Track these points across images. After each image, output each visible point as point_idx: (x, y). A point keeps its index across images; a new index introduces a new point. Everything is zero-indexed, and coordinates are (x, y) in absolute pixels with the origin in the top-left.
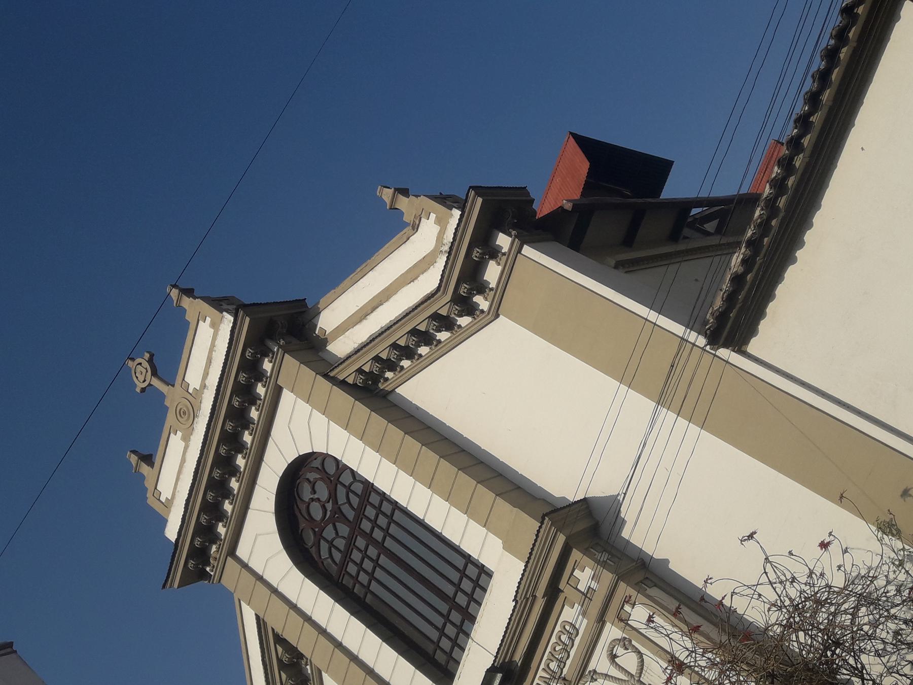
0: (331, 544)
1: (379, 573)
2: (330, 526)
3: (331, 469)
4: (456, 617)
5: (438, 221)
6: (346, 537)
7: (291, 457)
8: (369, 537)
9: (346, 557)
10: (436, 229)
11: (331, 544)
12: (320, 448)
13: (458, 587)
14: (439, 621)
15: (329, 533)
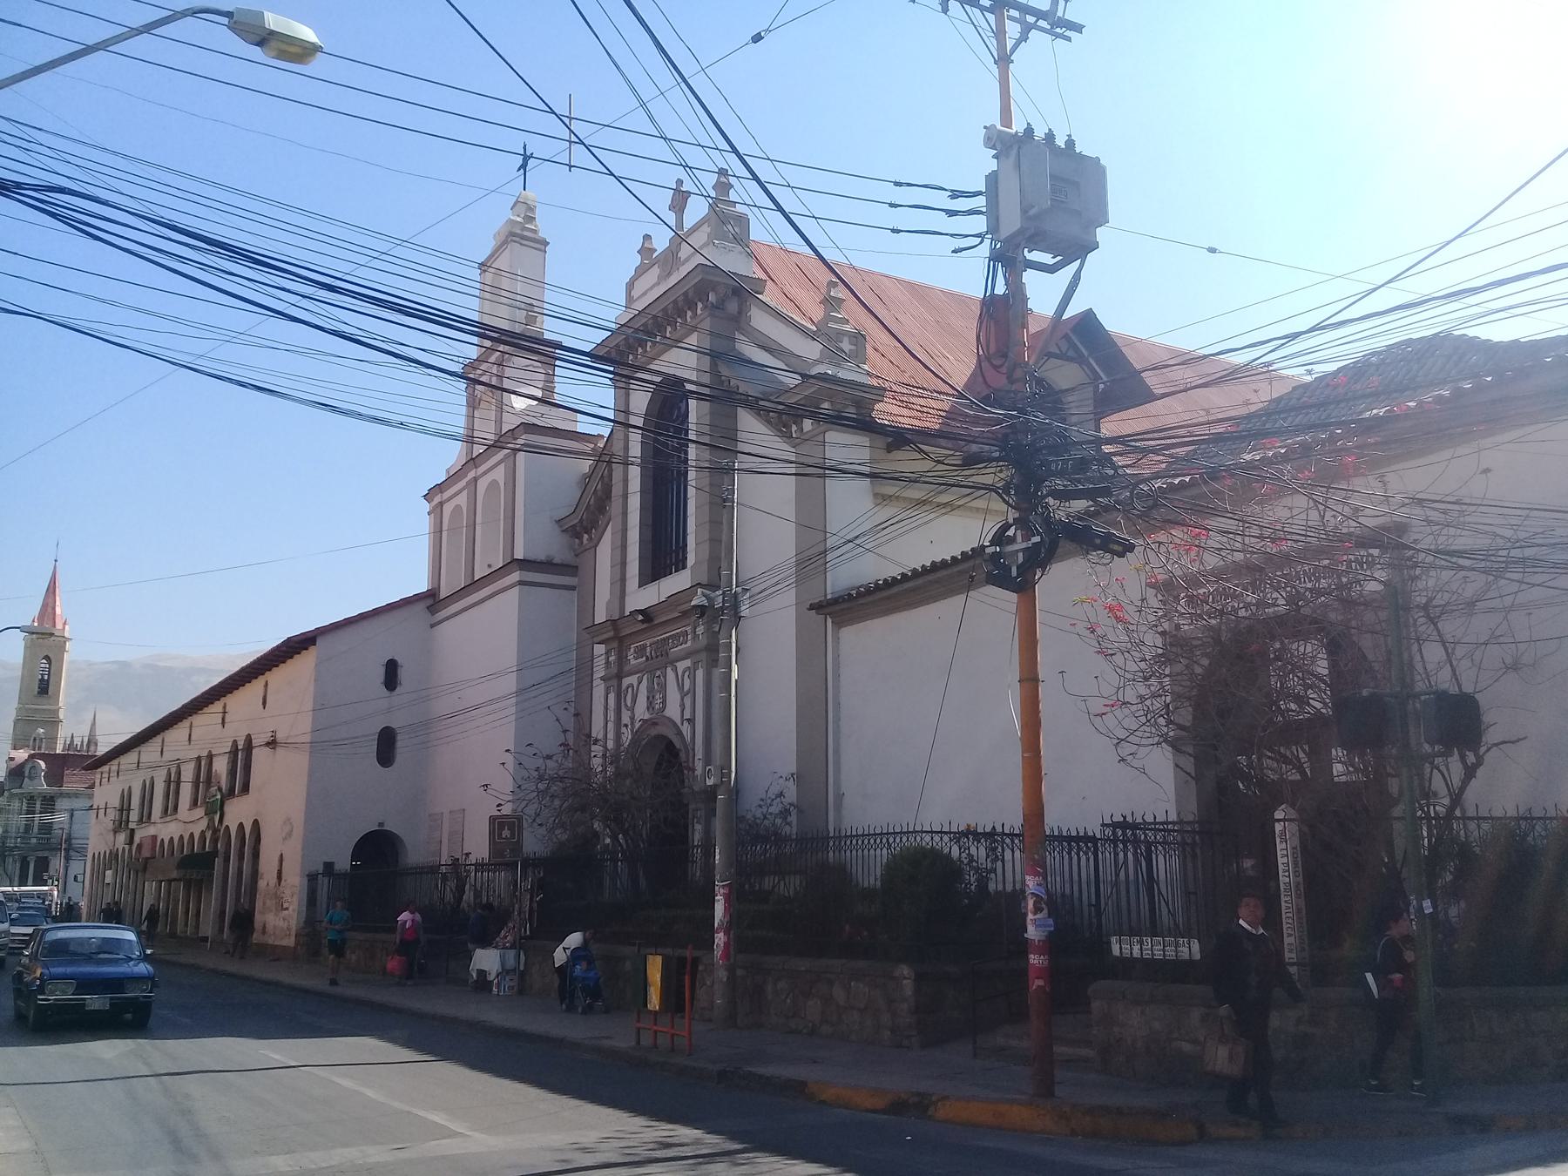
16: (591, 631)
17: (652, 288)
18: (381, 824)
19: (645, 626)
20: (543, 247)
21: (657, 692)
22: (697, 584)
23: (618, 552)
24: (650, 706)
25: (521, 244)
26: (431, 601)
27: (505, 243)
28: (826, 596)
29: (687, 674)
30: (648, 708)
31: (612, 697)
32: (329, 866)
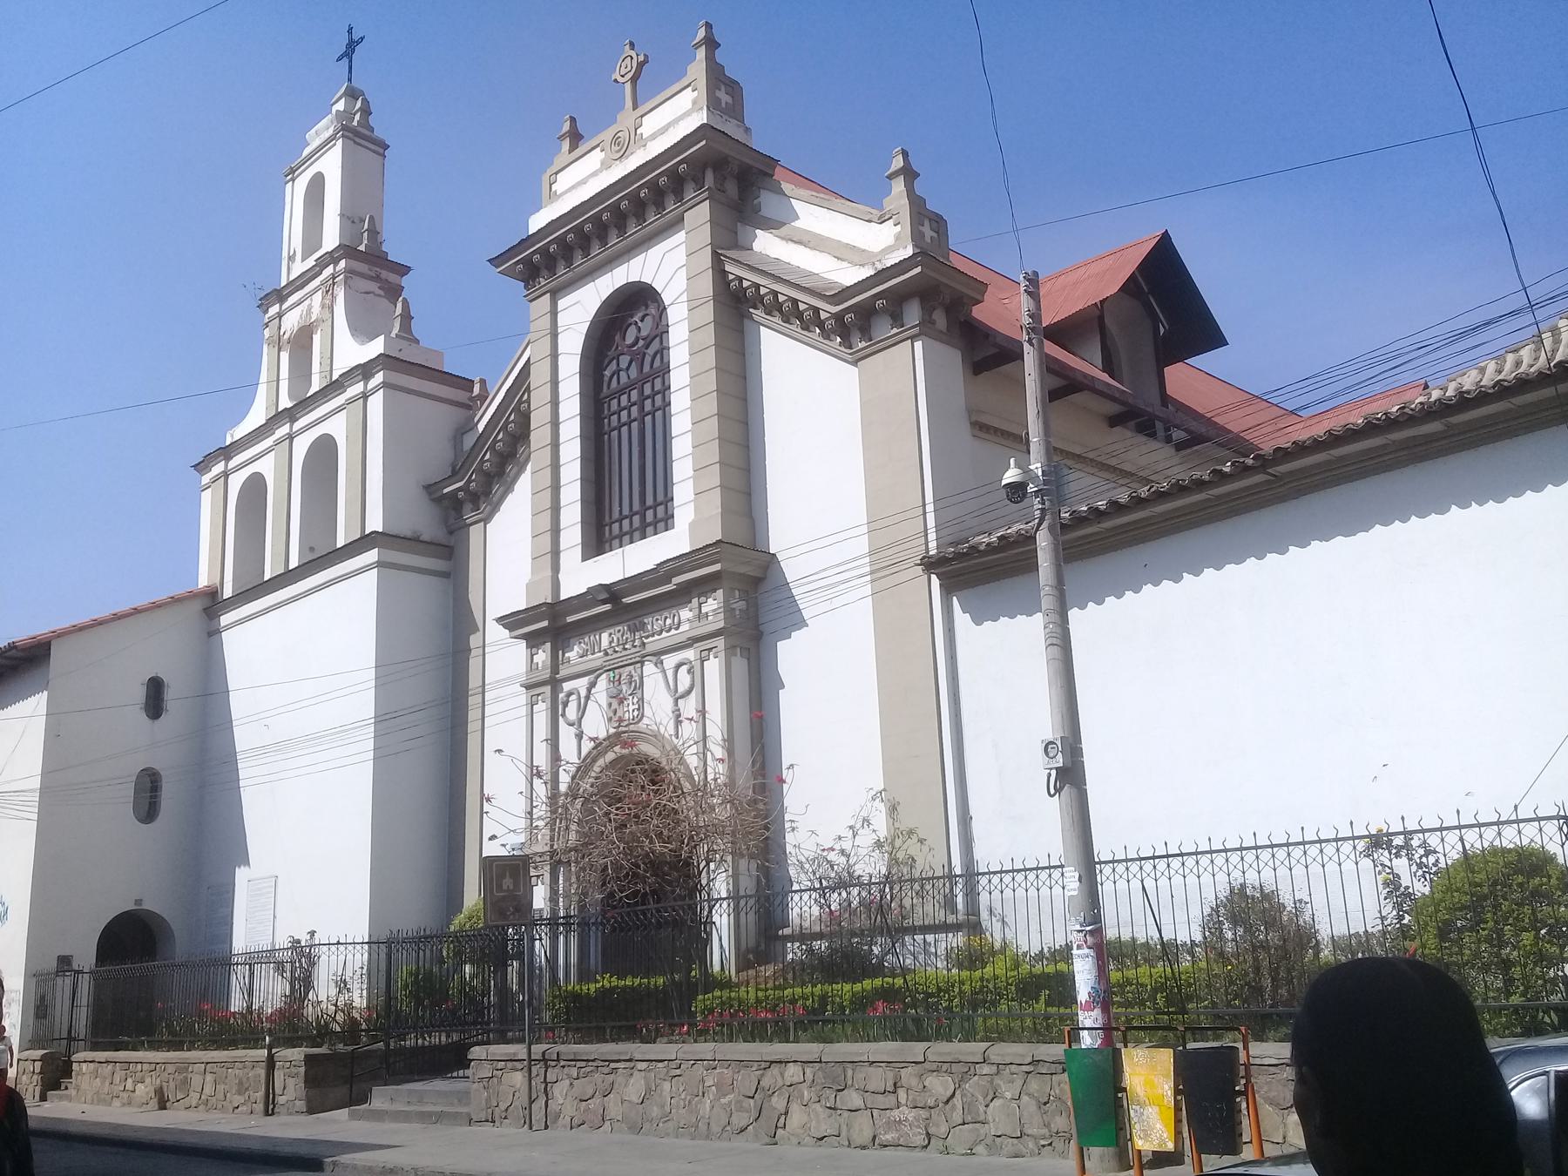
0: (617, 372)
1: (625, 429)
2: (629, 358)
3: (664, 323)
4: (636, 519)
5: (898, 237)
6: (632, 377)
7: (647, 279)
8: (643, 398)
9: (618, 392)
10: (891, 241)
11: (617, 372)
12: (667, 298)
13: (655, 507)
14: (626, 512)
15: (624, 361)
16: (511, 622)
17: (594, 174)
18: (138, 902)
19: (607, 607)
20: (381, 151)
21: (627, 690)
22: (719, 542)
23: (547, 516)
24: (613, 716)
25: (355, 142)
26: (212, 604)
27: (332, 138)
28: (927, 552)
29: (684, 669)
30: (610, 719)
31: (542, 709)
32: (64, 962)
